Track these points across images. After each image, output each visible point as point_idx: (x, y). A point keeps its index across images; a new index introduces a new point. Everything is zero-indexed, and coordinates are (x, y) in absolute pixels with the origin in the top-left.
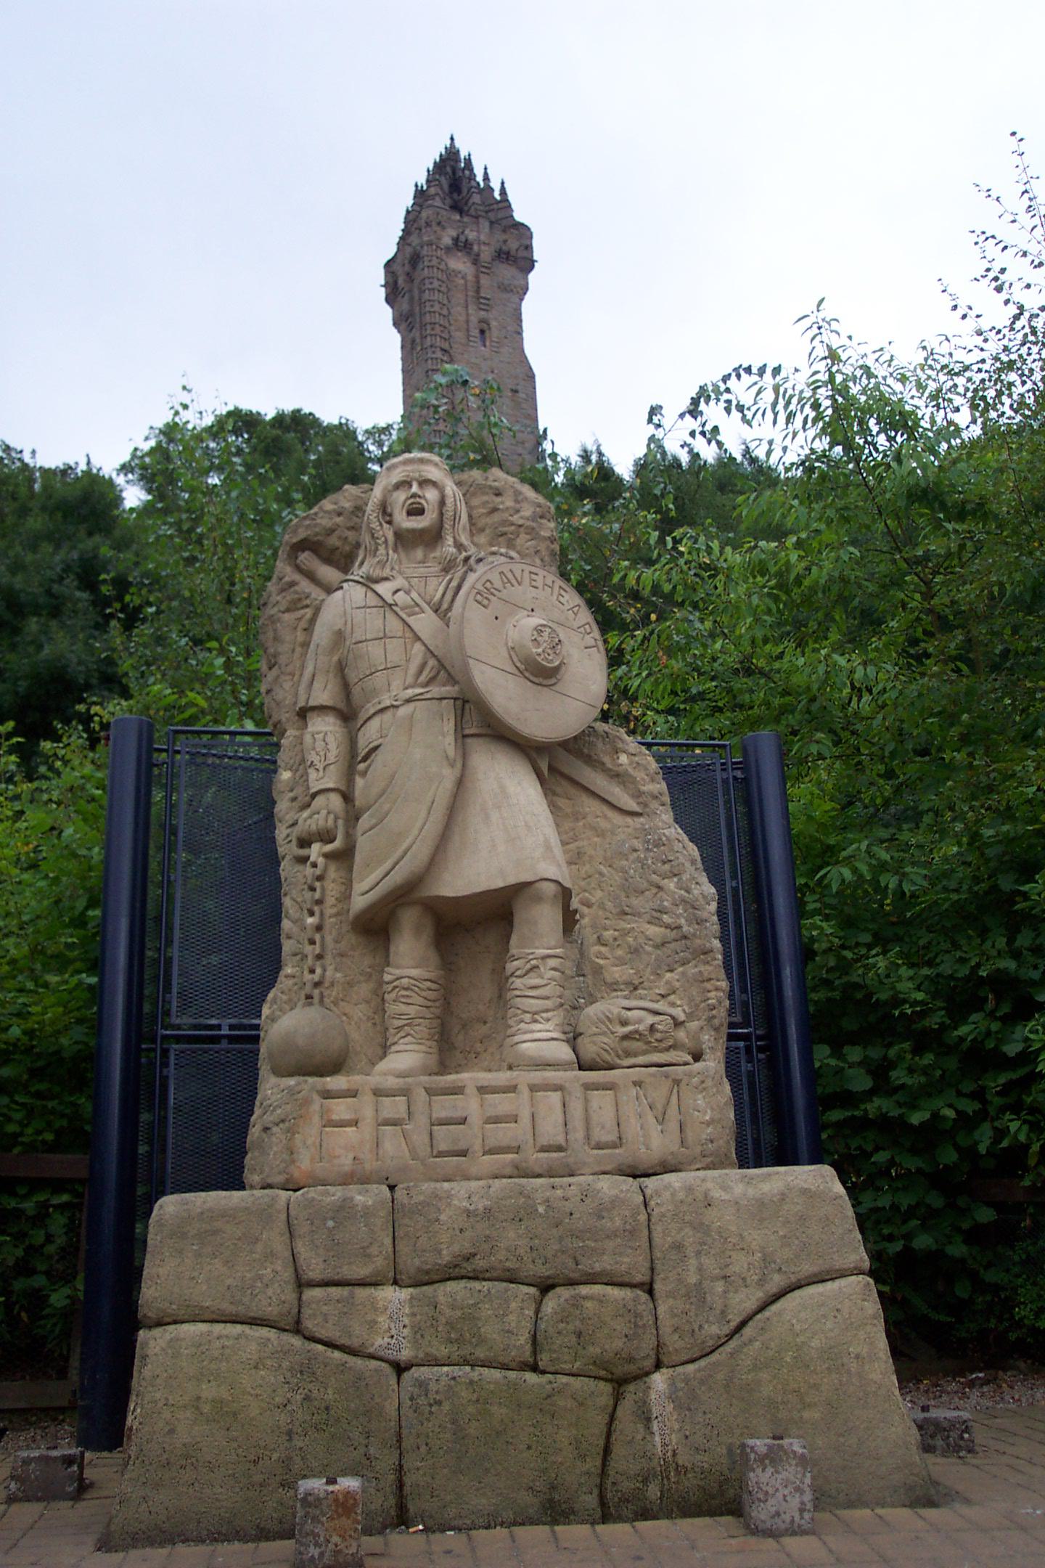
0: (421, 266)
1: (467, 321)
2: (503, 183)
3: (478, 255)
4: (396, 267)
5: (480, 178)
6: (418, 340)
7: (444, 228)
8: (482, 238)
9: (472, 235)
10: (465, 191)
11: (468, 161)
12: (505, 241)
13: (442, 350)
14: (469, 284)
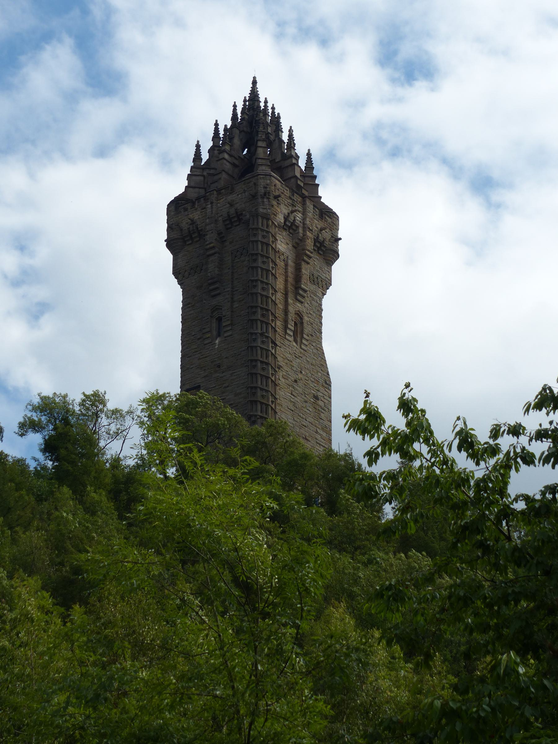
2: (309, 155)
9: (299, 217)
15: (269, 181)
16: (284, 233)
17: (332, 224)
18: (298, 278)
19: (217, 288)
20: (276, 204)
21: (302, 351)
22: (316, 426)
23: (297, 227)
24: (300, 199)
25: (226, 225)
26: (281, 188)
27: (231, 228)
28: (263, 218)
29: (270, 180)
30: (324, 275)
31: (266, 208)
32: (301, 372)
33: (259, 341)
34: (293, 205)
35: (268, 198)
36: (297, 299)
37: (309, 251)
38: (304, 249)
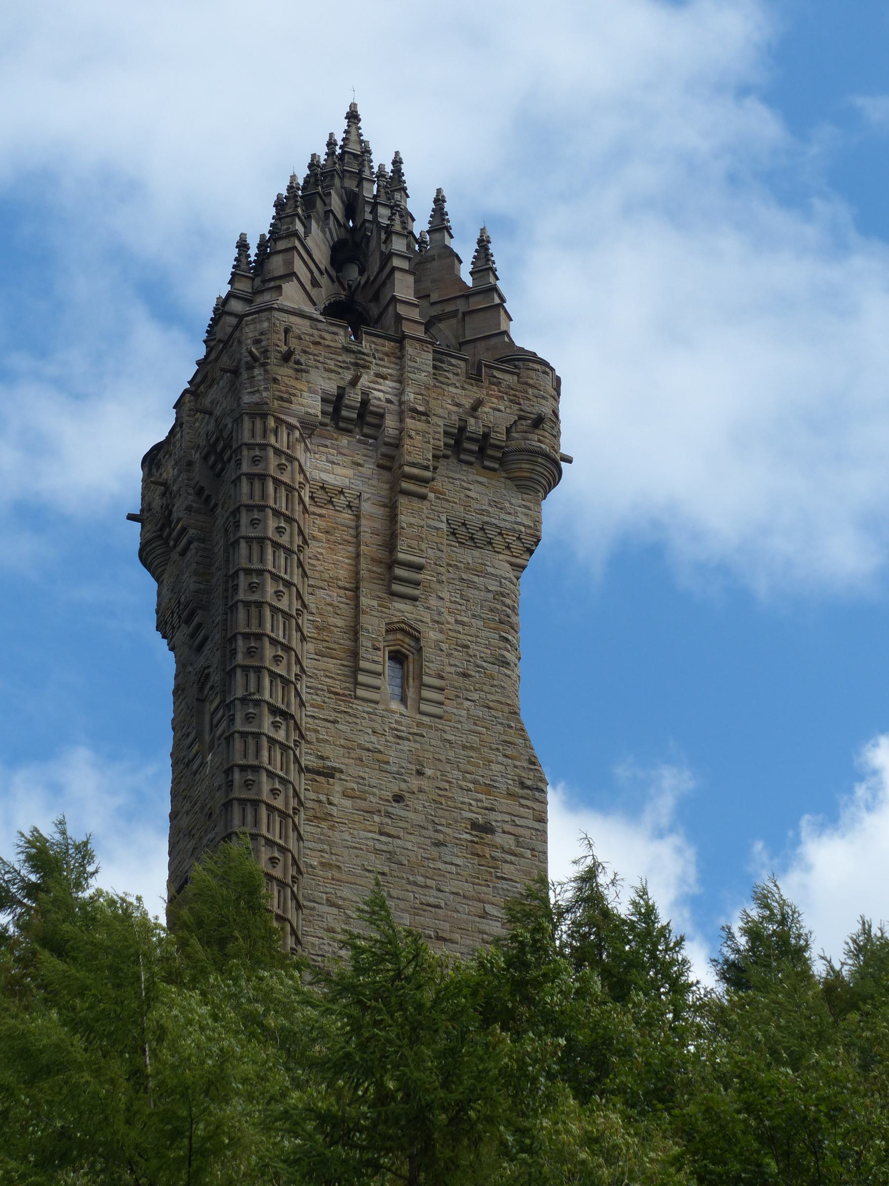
0: (230, 474)
1: (355, 631)
2: (483, 244)
3: (397, 445)
4: (168, 472)
5: (420, 225)
6: (215, 678)
7: (300, 370)
8: (410, 396)
9: (382, 392)
10: (374, 266)
11: (394, 182)
12: (477, 405)
13: (275, 711)
14: (366, 525)
15: (266, 324)
16: (344, 441)
17: (520, 387)
18: (390, 541)
19: (199, 625)
20: (291, 372)
21: (426, 719)
22: (479, 900)
23: (382, 416)
24: (388, 346)
25: (213, 467)
26: (311, 331)
27: (222, 470)
28: (252, 416)
29: (268, 319)
30: (508, 517)
31: (258, 391)
32: (420, 773)
33: (239, 717)
34: (356, 365)
35: (264, 365)
36: (394, 594)
37: (413, 465)
38: (401, 466)
